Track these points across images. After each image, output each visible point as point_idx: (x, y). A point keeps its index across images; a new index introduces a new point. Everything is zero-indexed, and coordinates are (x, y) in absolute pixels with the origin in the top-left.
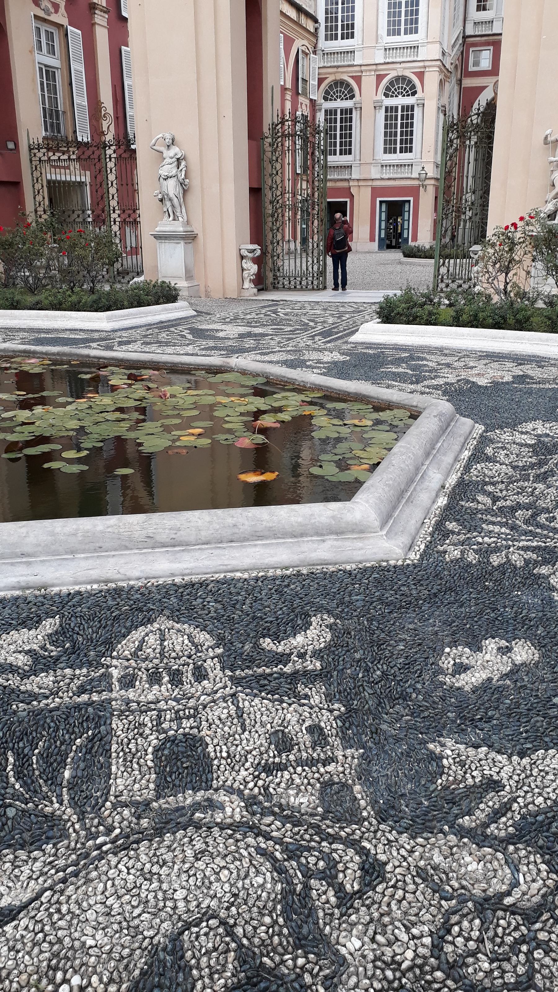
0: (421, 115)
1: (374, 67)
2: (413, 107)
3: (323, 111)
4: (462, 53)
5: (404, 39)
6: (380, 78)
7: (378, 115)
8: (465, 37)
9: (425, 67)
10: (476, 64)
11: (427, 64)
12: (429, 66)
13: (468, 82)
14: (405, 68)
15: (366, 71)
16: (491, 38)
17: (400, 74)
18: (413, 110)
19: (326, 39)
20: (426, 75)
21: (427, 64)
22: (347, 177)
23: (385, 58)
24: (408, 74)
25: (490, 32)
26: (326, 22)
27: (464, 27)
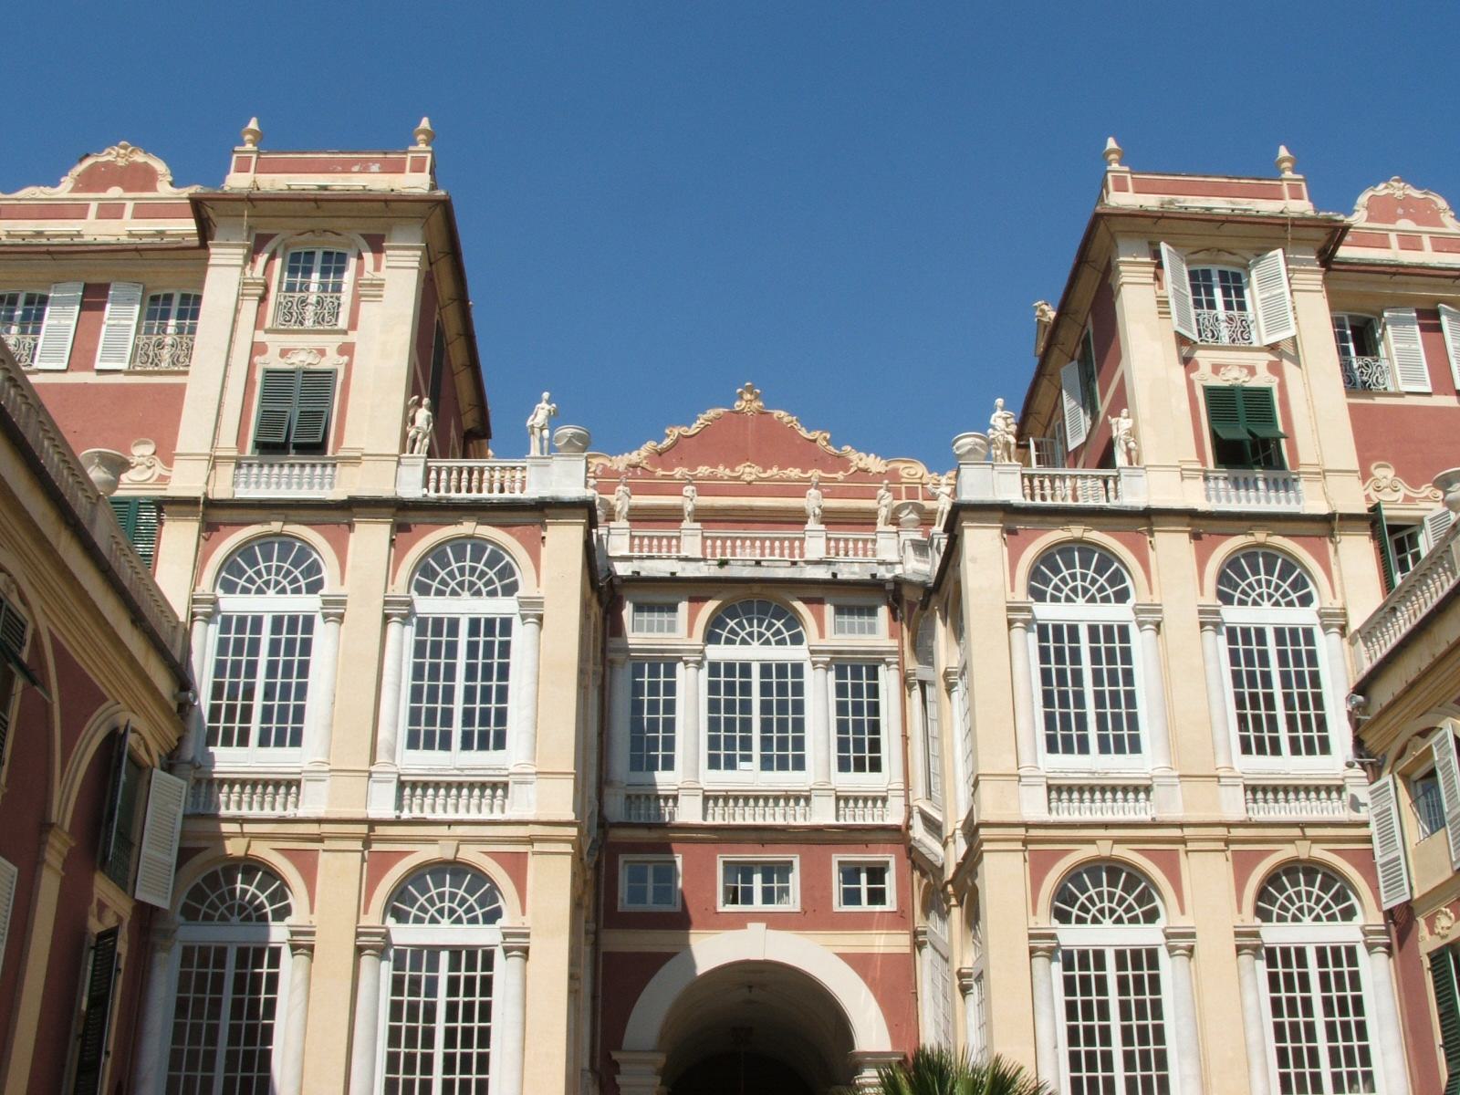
0: (514, 980)
5: (456, 761)
8: (603, 824)
10: (637, 895)
18: (488, 963)
20: (532, 862)
23: (399, 807)
24: (470, 854)
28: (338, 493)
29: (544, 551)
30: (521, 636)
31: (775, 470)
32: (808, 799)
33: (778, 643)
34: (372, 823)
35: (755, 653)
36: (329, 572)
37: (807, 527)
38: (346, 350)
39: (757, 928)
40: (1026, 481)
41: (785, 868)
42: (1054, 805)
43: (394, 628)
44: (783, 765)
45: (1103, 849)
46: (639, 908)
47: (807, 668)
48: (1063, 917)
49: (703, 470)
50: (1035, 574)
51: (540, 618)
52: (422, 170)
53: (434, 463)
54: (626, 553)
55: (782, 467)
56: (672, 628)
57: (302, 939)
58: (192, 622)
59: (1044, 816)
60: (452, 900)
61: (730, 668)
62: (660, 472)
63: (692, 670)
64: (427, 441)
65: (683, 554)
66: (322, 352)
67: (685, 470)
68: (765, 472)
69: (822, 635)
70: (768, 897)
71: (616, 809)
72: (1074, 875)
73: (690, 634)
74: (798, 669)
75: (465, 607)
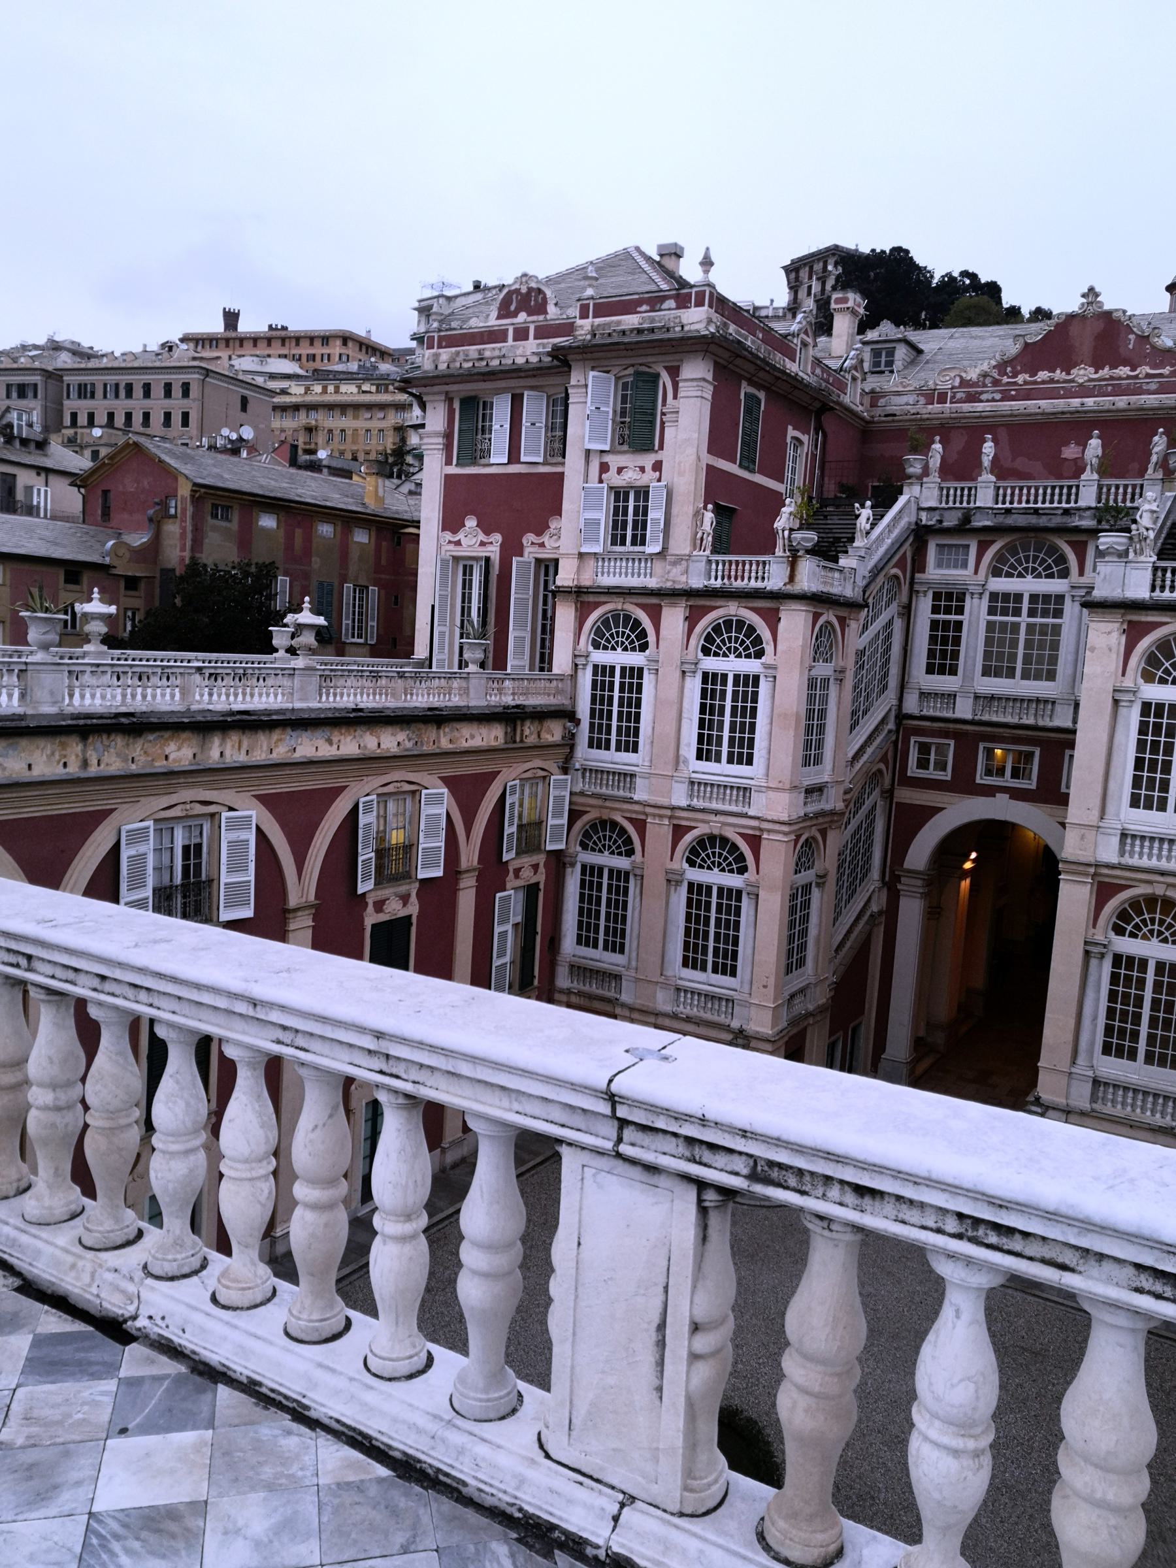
0: (752, 913)
1: (668, 813)
2: (739, 893)
3: (578, 867)
4: (896, 743)
5: (722, 770)
6: (679, 832)
7: (674, 897)
8: (901, 717)
9: (761, 830)
11: (765, 825)
12: (769, 831)
13: (906, 795)
14: (724, 824)
15: (654, 816)
16: (951, 726)
17: (716, 832)
19: (591, 746)
21: (765, 825)
22: (611, 994)
24: (730, 833)
25: (949, 715)
26: (592, 716)
27: (901, 699)
28: (652, 583)
29: (782, 626)
30: (764, 688)
31: (1107, 369)
32: (1054, 703)
33: (1047, 576)
34: (673, 808)
35: (1028, 585)
36: (651, 638)
37: (1083, 477)
38: (658, 466)
39: (1002, 798)
40: (1159, 574)
41: (1032, 753)
42: (1128, 848)
43: (688, 680)
44: (1038, 677)
45: (1159, 890)
46: (922, 774)
47: (1068, 600)
48: (1119, 931)
49: (1043, 375)
50: (1152, 660)
51: (775, 677)
52: (702, 305)
53: (714, 558)
54: (933, 503)
55: (1114, 366)
56: (965, 565)
57: (638, 872)
58: (576, 672)
59: (1114, 859)
60: (720, 857)
61: (1006, 596)
62: (1005, 379)
63: (976, 601)
64: (710, 539)
65: (978, 504)
66: (642, 469)
67: (1027, 377)
68: (1096, 372)
69: (1081, 573)
70: (1015, 774)
71: (911, 705)
72: (1135, 904)
73: (976, 572)
74: (1060, 598)
75: (732, 665)
